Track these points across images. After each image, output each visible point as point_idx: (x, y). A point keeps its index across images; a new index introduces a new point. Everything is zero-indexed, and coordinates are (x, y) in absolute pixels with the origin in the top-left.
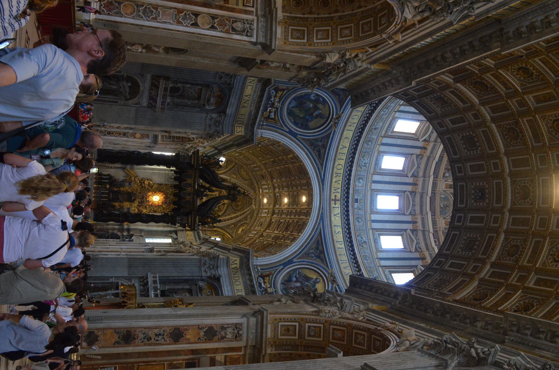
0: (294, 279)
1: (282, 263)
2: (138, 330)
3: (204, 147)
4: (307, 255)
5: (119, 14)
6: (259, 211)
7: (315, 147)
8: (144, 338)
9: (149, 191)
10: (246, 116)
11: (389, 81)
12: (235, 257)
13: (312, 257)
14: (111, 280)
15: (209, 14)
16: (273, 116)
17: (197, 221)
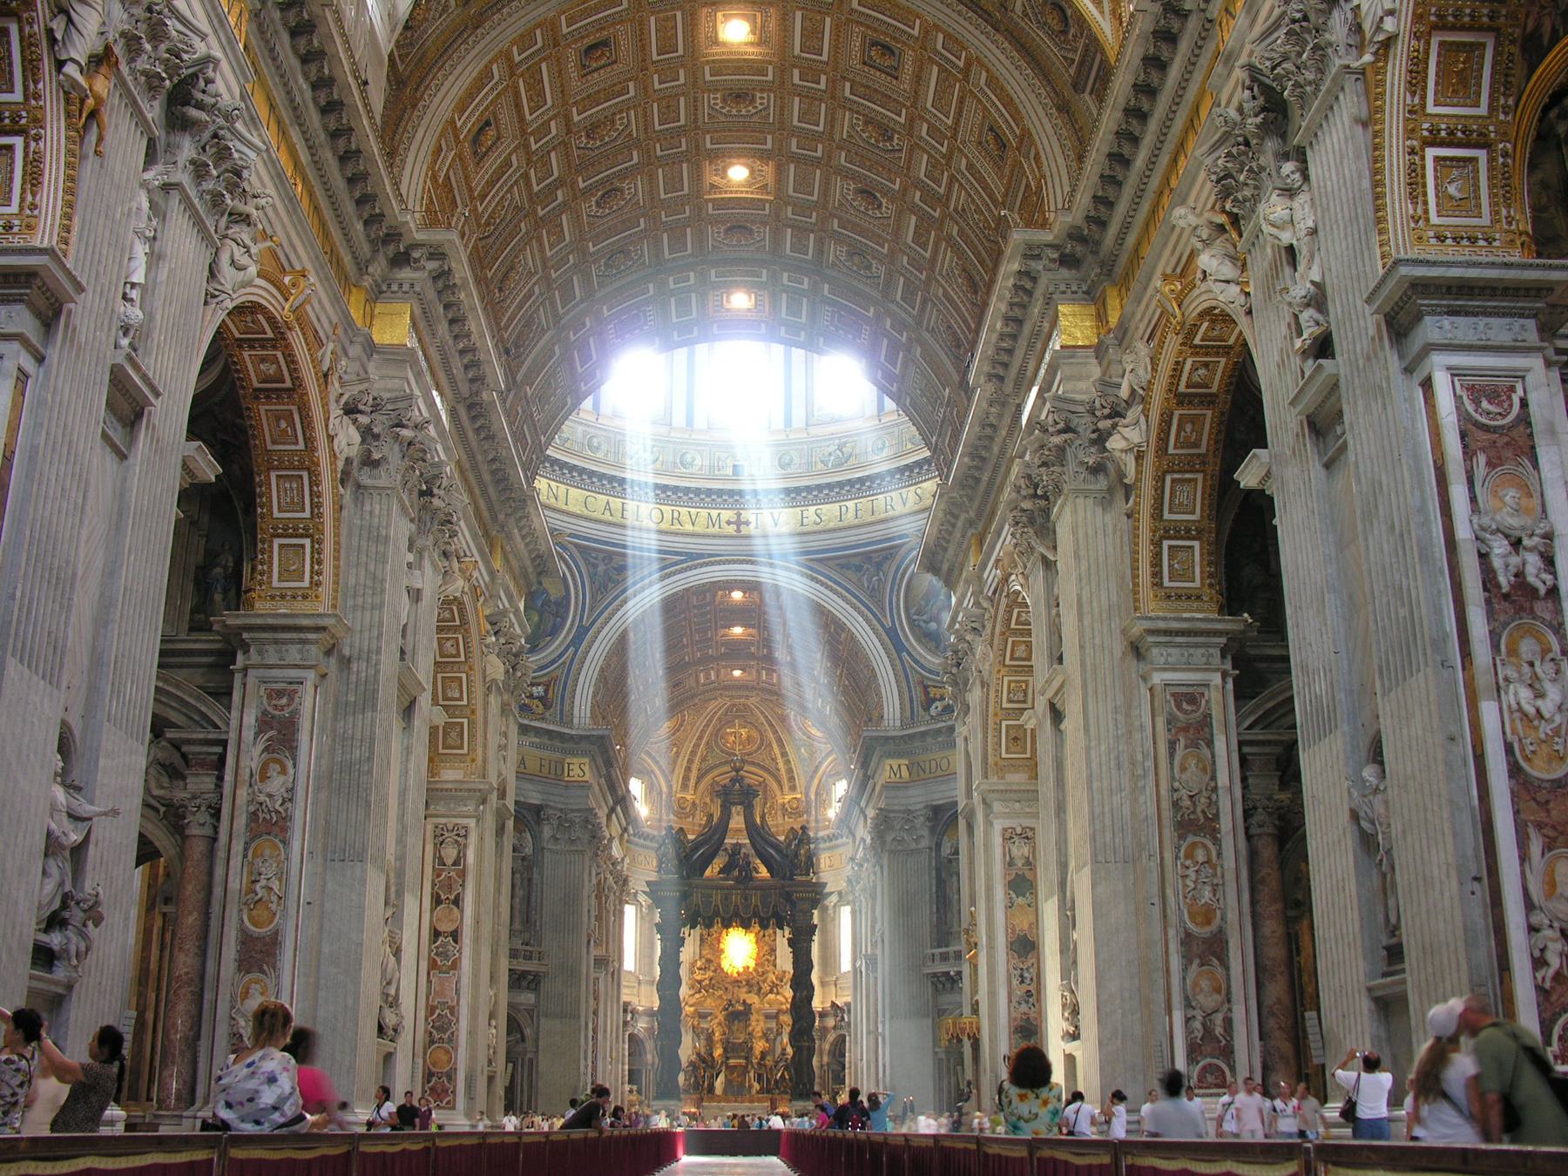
0: (933, 625)
1: (895, 655)
2: (1014, 1015)
3: (611, 839)
4: (875, 593)
5: (451, 1076)
6: (762, 690)
7: (610, 579)
8: (1027, 1002)
9: (719, 967)
10: (546, 754)
11: (520, 530)
12: (883, 769)
13: (880, 580)
14: (943, 1056)
15: (432, 911)
16: (541, 689)
17: (804, 878)
